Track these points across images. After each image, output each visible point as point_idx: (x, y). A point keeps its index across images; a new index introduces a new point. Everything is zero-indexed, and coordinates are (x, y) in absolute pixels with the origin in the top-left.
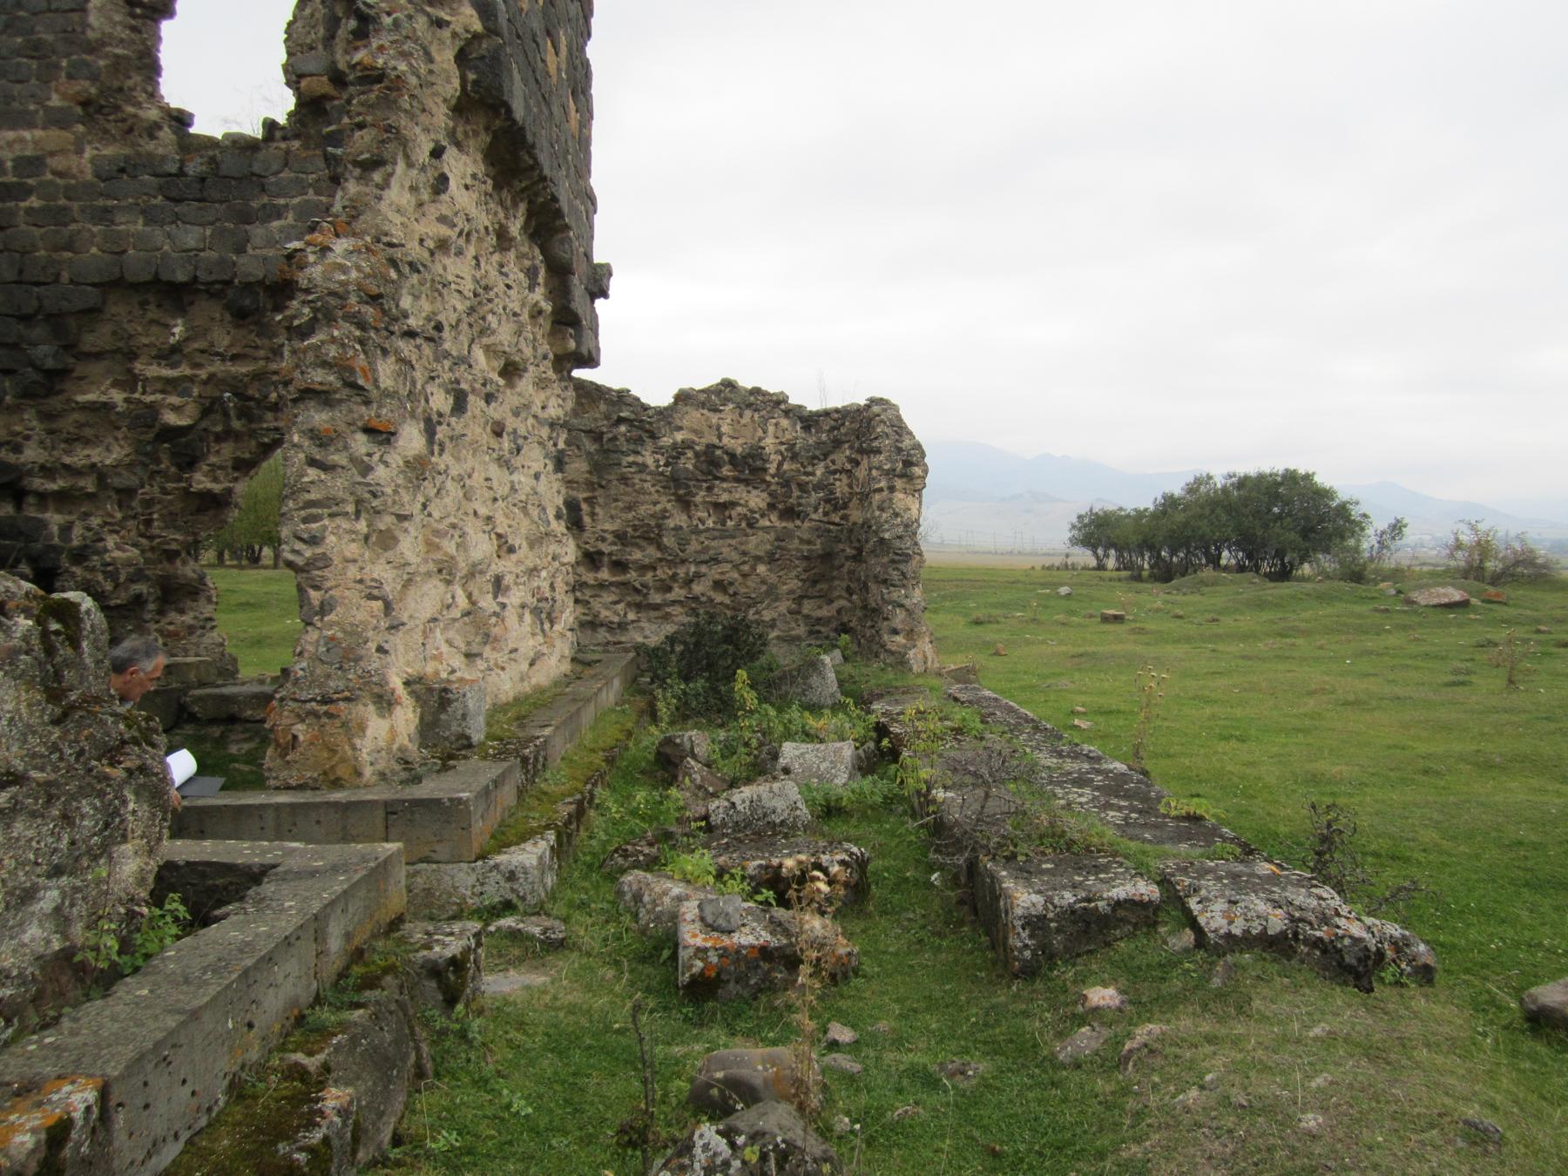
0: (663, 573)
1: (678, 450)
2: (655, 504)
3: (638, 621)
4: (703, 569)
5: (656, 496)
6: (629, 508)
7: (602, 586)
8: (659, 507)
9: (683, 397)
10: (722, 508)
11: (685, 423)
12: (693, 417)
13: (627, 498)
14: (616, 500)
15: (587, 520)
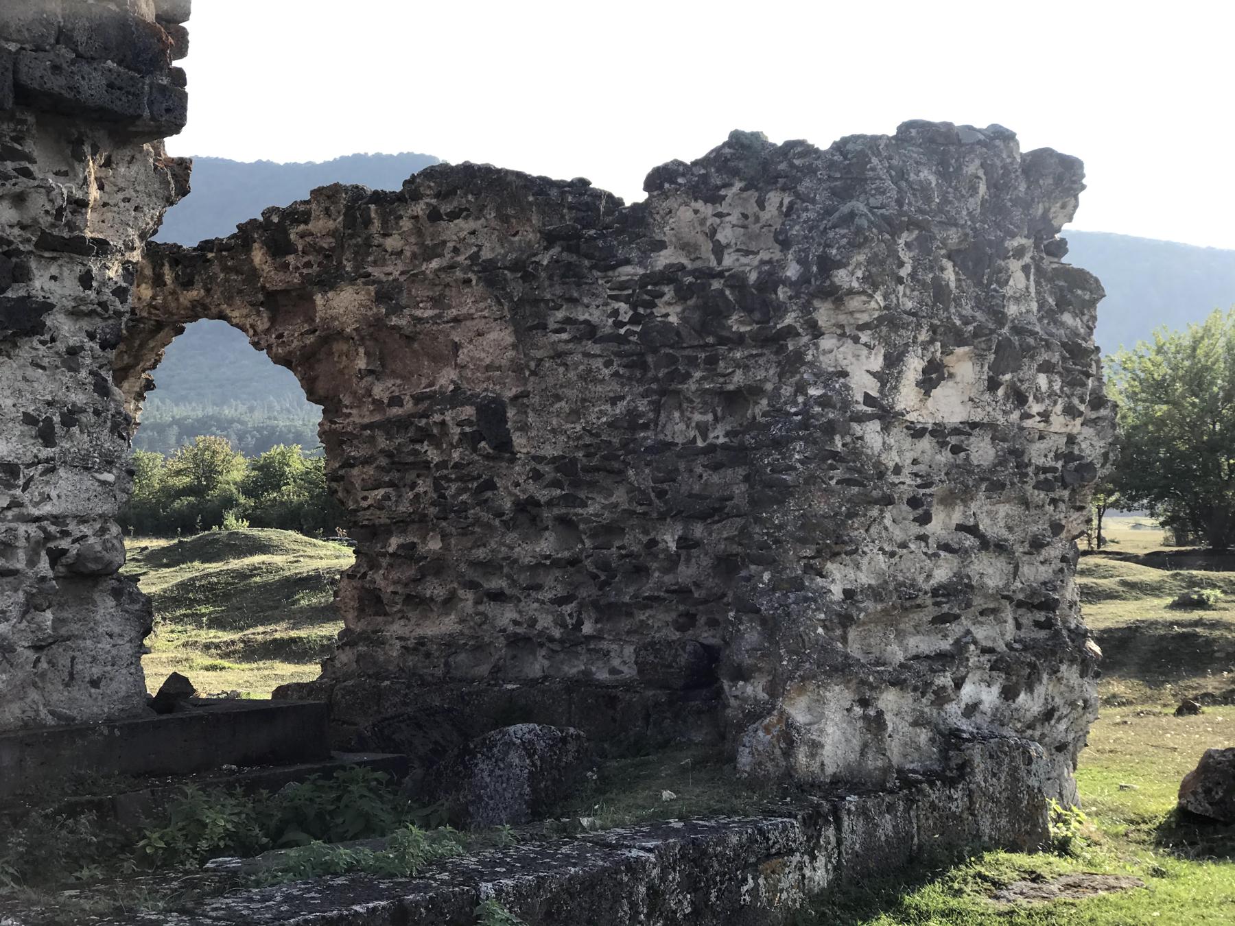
0: (633, 540)
1: (643, 294)
2: (614, 401)
3: (598, 637)
4: (698, 530)
5: (615, 387)
6: (575, 414)
7: (542, 565)
8: (620, 408)
9: (660, 179)
10: (734, 400)
11: (667, 235)
12: (685, 216)
13: (571, 393)
14: (558, 398)
15: (518, 440)
